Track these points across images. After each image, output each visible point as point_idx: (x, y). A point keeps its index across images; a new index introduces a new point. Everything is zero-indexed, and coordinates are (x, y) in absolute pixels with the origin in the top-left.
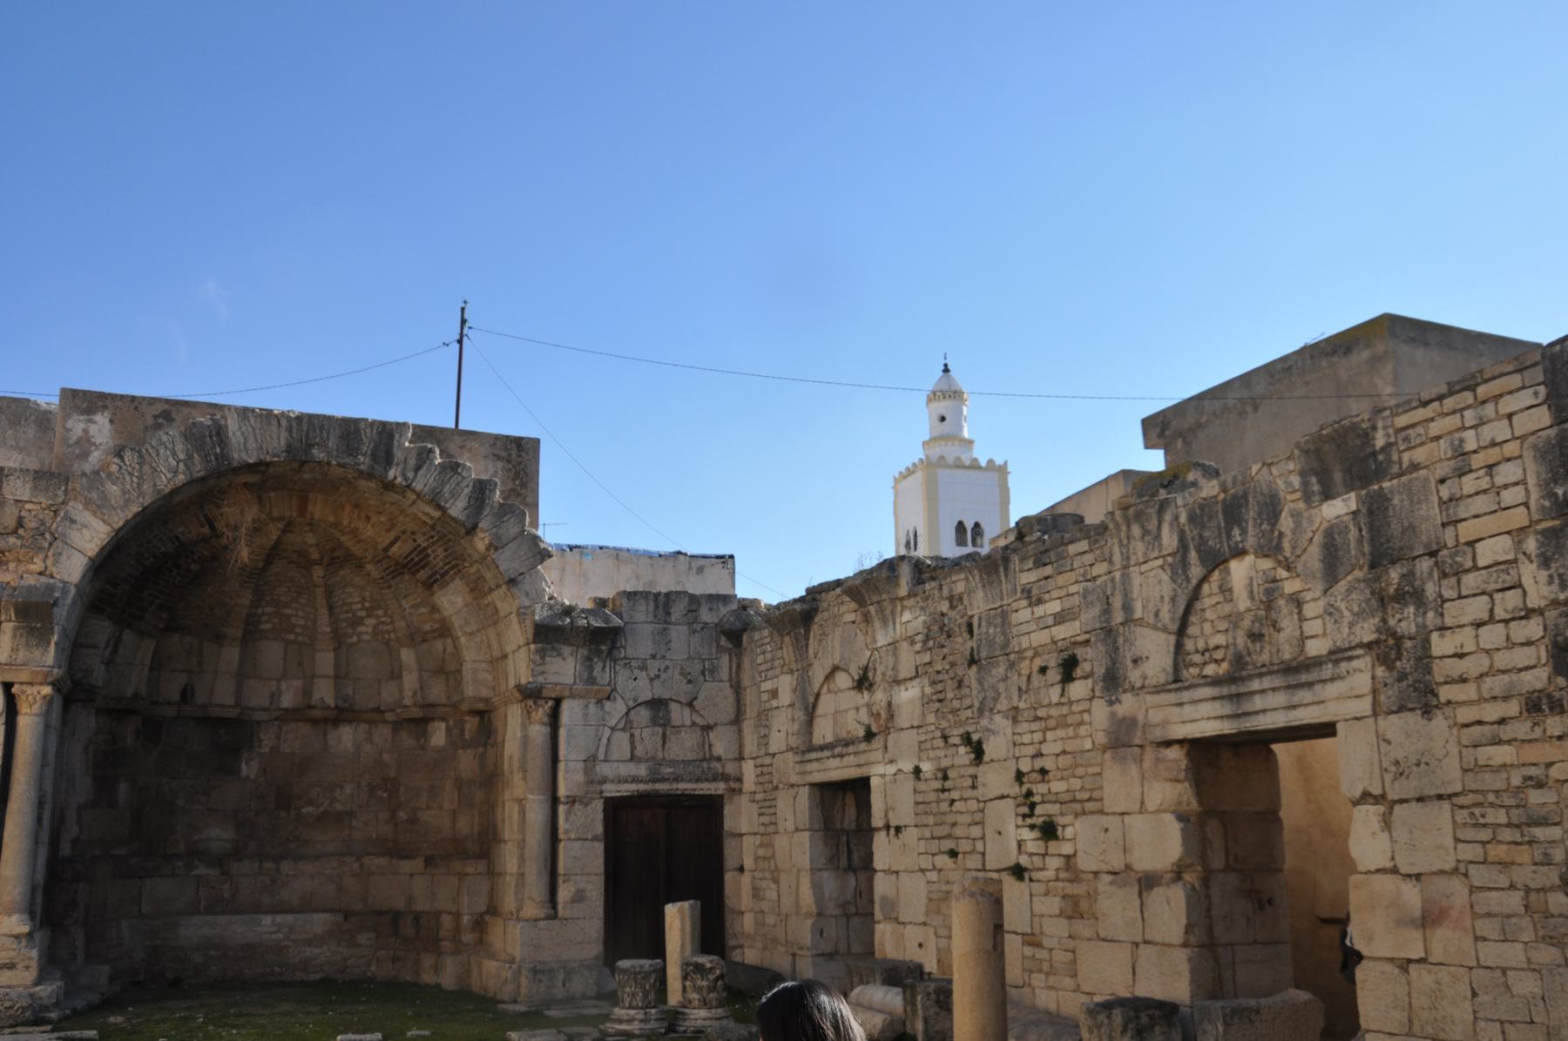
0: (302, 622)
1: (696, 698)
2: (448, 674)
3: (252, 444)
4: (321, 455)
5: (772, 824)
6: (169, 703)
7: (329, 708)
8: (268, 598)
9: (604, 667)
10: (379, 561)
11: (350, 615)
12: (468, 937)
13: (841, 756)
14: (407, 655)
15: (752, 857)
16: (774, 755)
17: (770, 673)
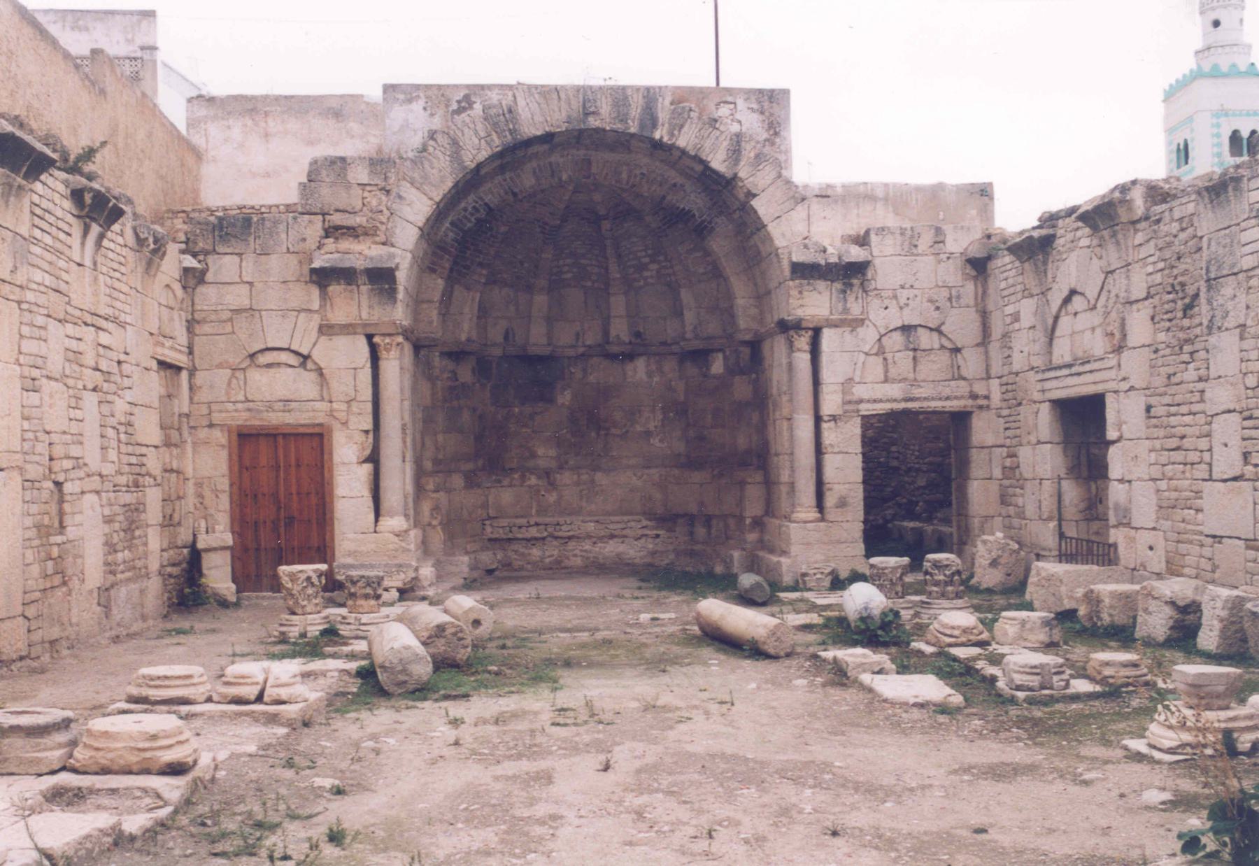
1: (943, 323)
3: (539, 118)
5: (1016, 437)
7: (625, 344)
8: (567, 251)
9: (857, 298)
13: (1079, 374)
15: (1000, 467)
16: (1017, 374)
17: (1013, 299)
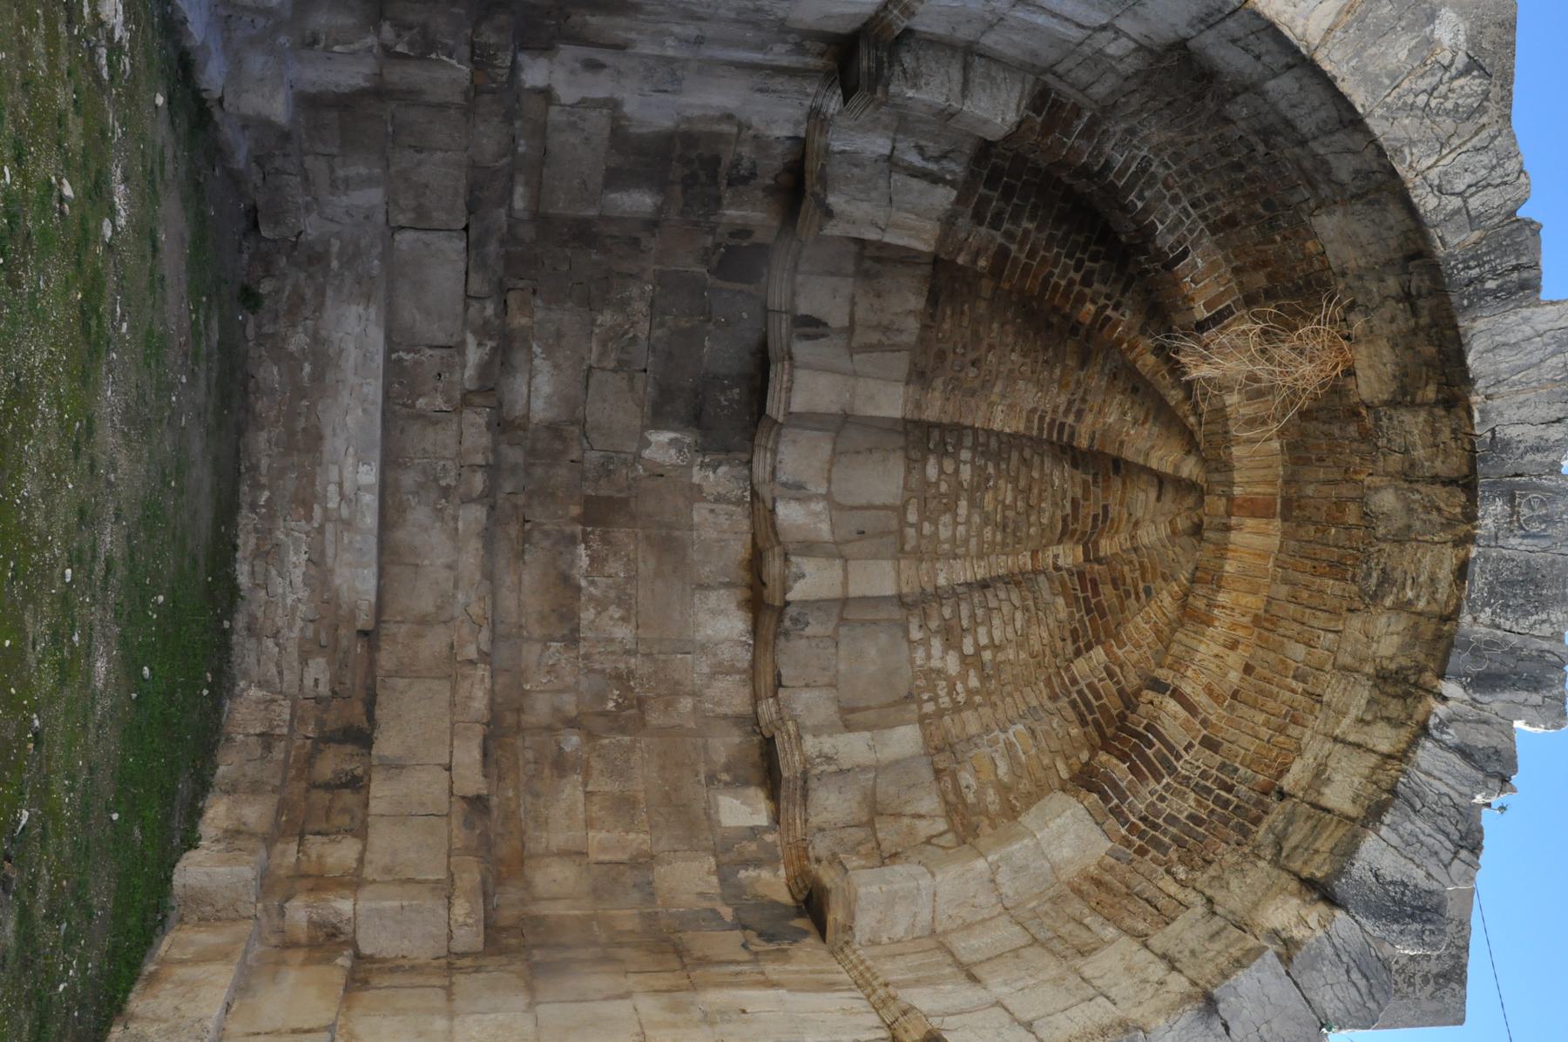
0: (944, 533)
2: (871, 823)
4: (1489, 521)
6: (794, 294)
8: (991, 470)
10: (1111, 675)
11: (965, 623)
12: (299, 913)
14: (905, 739)
